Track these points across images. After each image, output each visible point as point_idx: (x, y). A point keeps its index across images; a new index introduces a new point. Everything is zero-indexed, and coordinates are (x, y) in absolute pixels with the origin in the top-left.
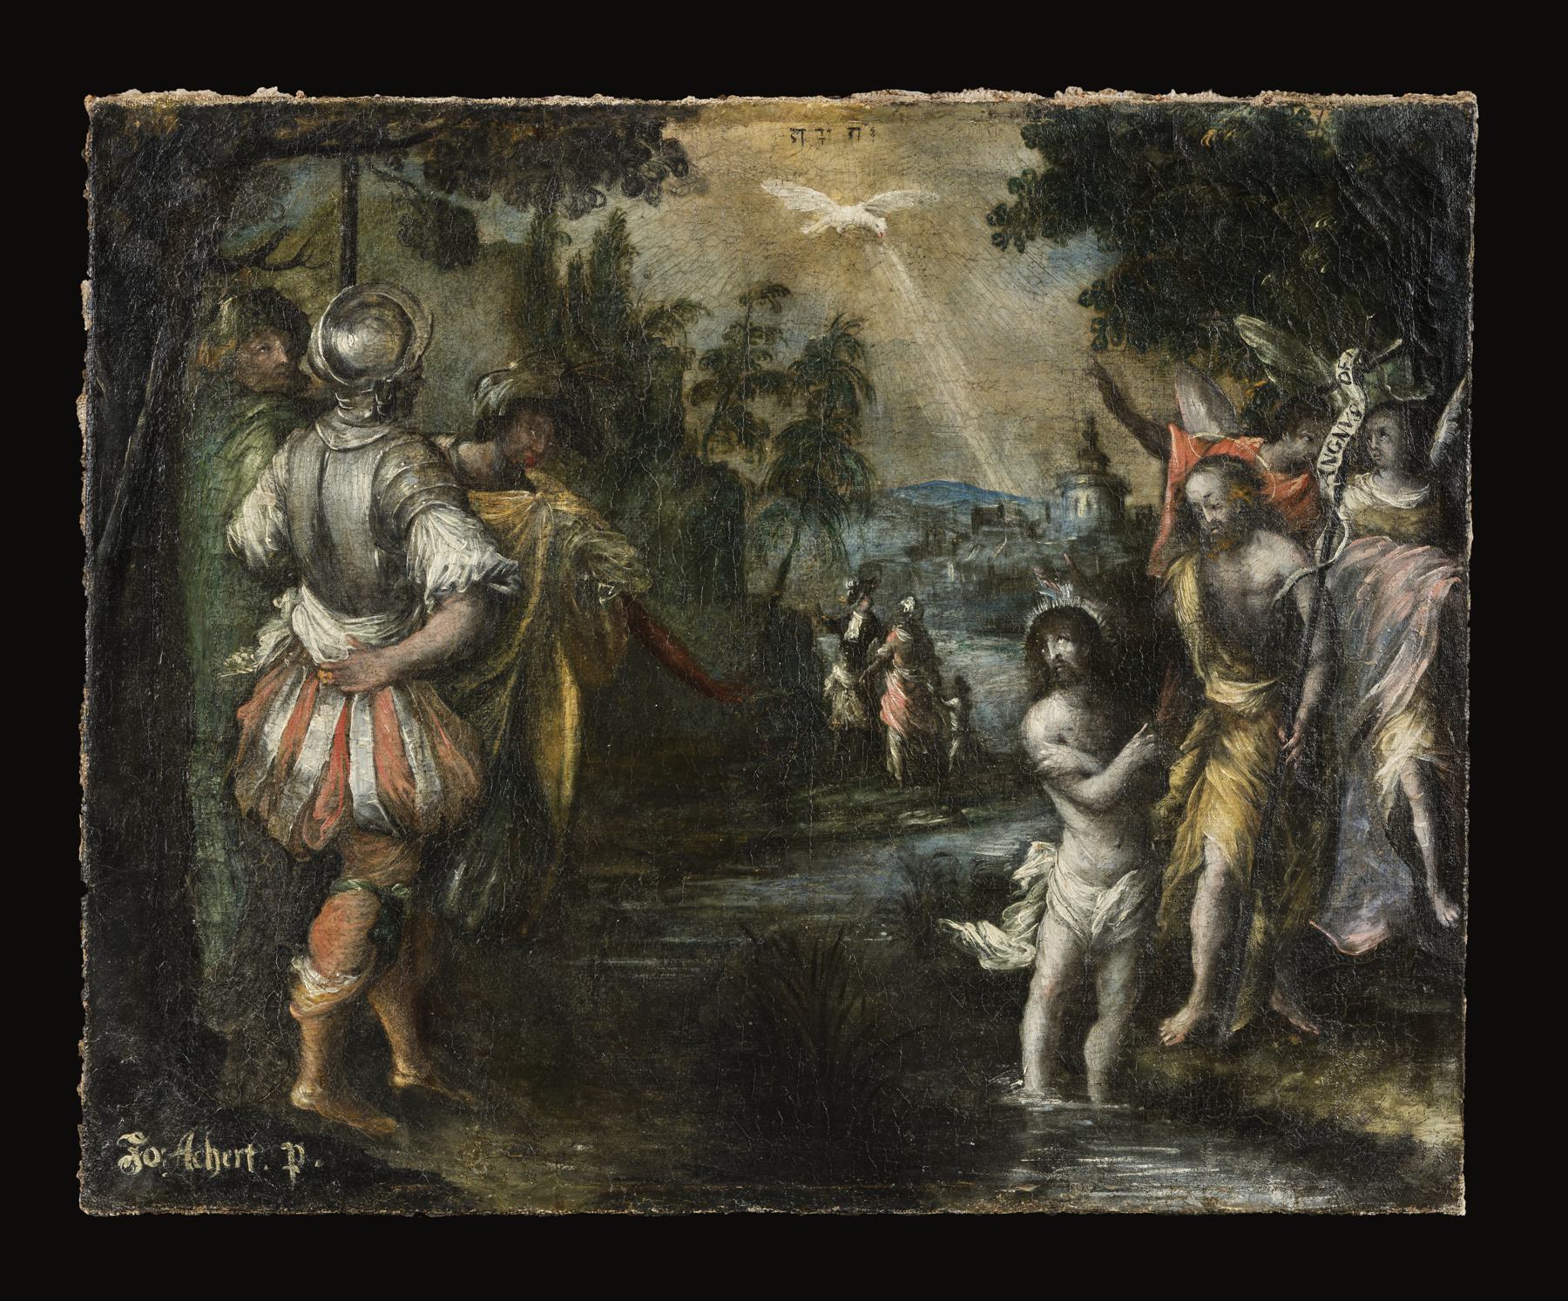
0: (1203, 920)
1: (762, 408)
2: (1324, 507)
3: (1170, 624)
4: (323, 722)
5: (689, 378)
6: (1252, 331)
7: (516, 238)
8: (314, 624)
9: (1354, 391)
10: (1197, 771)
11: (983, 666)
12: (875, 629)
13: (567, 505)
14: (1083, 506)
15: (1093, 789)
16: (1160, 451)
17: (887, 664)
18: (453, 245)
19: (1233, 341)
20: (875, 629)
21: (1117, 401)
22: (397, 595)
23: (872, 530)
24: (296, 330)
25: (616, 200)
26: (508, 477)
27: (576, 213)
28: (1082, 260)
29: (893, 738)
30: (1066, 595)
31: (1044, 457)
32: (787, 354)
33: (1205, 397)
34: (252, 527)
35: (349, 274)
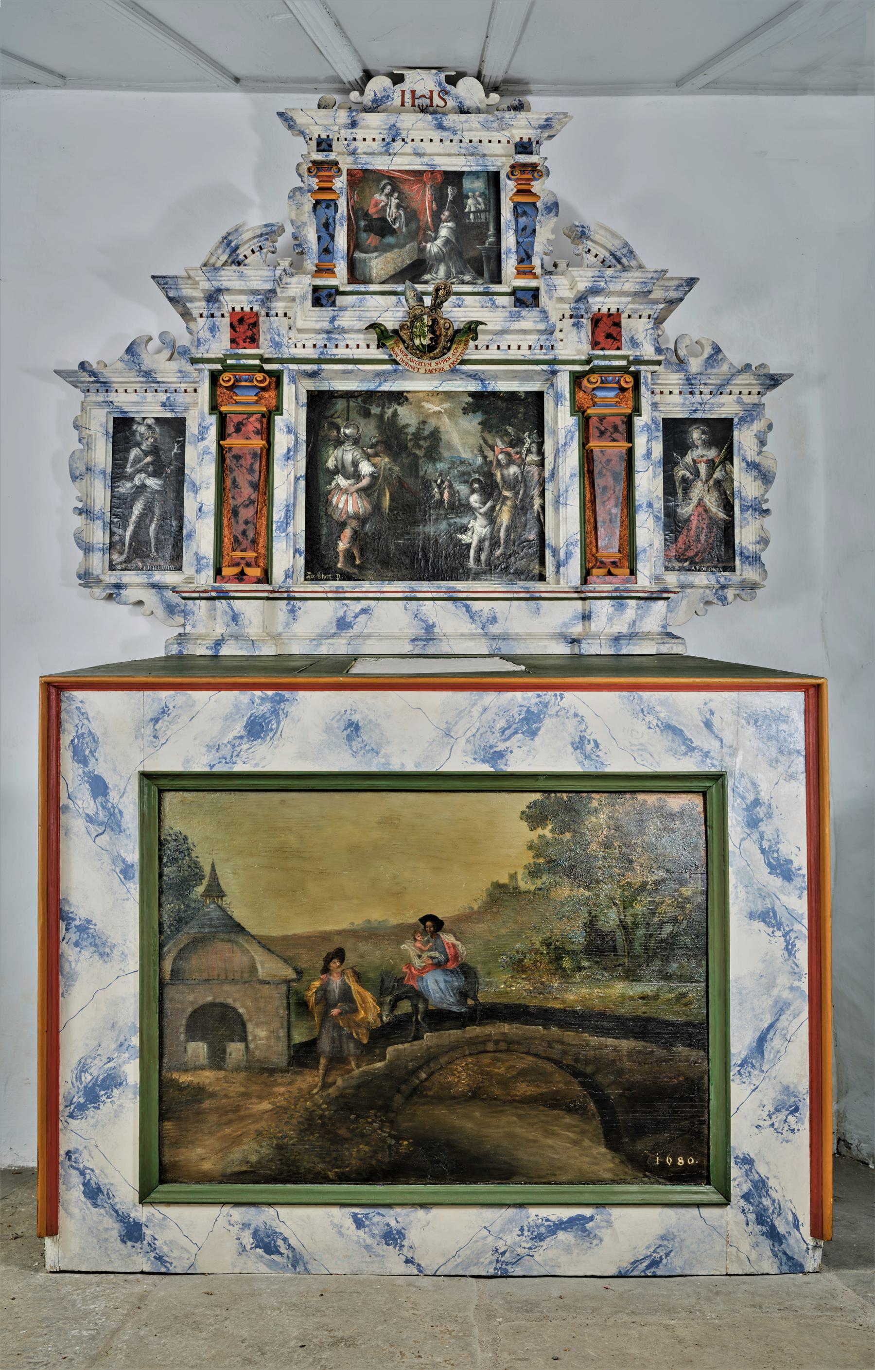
0: (502, 534)
1: (422, 443)
2: (523, 460)
4: (343, 498)
5: (409, 437)
6: (510, 429)
10: (501, 507)
11: (462, 489)
12: (442, 482)
13: (387, 460)
14: (479, 460)
15: (482, 510)
18: (367, 414)
19: (506, 430)
20: (442, 482)
22: (357, 476)
23: (442, 464)
24: (338, 429)
25: (396, 406)
26: (376, 455)
27: (388, 408)
28: (478, 417)
30: (477, 476)
31: (473, 451)
32: (426, 433)
34: (331, 464)
35: (348, 419)
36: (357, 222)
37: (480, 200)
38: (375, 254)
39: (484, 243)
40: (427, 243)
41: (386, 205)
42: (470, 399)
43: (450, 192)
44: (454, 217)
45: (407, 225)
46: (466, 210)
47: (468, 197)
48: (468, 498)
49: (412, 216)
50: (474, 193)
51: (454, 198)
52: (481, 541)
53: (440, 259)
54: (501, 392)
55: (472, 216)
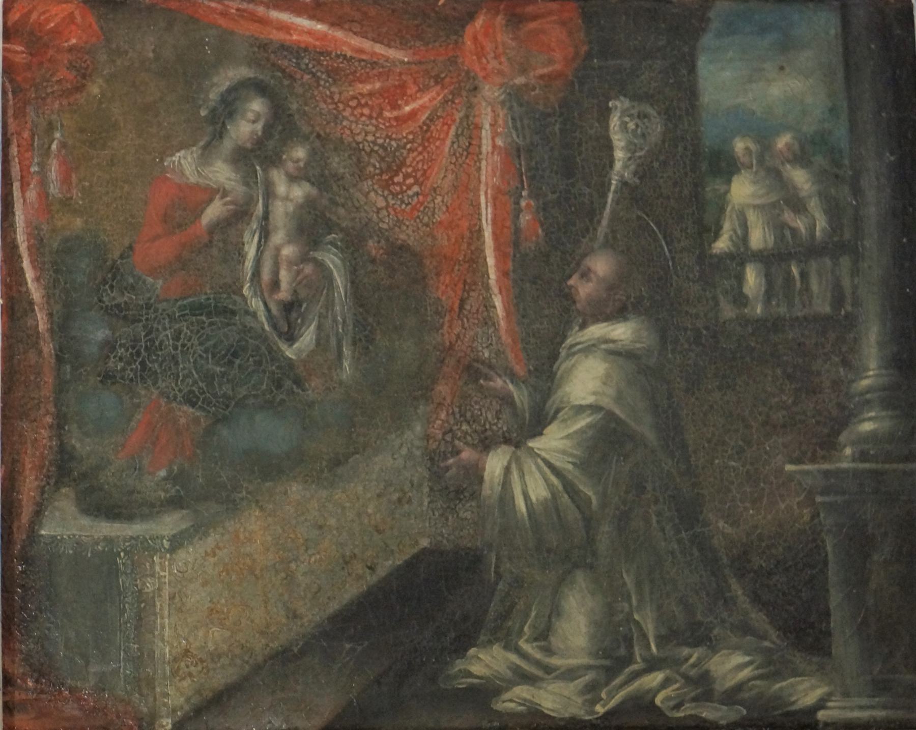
36: (62, 326)
37: (800, 178)
38: (169, 524)
39: (828, 445)
40: (486, 445)
41: (240, 214)
43: (624, 136)
44: (646, 291)
45: (364, 341)
46: (722, 245)
47: (725, 166)
49: (395, 285)
50: (765, 138)
51: (645, 172)
53: (565, 544)
55: (752, 279)
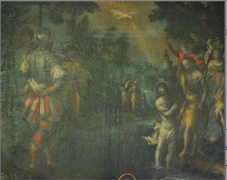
2: (206, 66)
3: (180, 86)
4: (35, 102)
6: (193, 35)
7: (69, 19)
8: (35, 85)
9: (210, 46)
10: (185, 110)
14: (165, 65)
15: (167, 113)
16: (178, 56)
17: (132, 92)
18: (58, 20)
21: (171, 48)
22: (48, 80)
23: (130, 69)
24: (31, 35)
25: (86, 13)
26: (67, 60)
27: (79, 14)
28: (164, 24)
29: (133, 105)
30: (162, 80)
33: (186, 47)
34: (23, 67)
35: (40, 25)
42: (157, 7)
48: (154, 102)
52: (166, 142)
54: (185, 2)
